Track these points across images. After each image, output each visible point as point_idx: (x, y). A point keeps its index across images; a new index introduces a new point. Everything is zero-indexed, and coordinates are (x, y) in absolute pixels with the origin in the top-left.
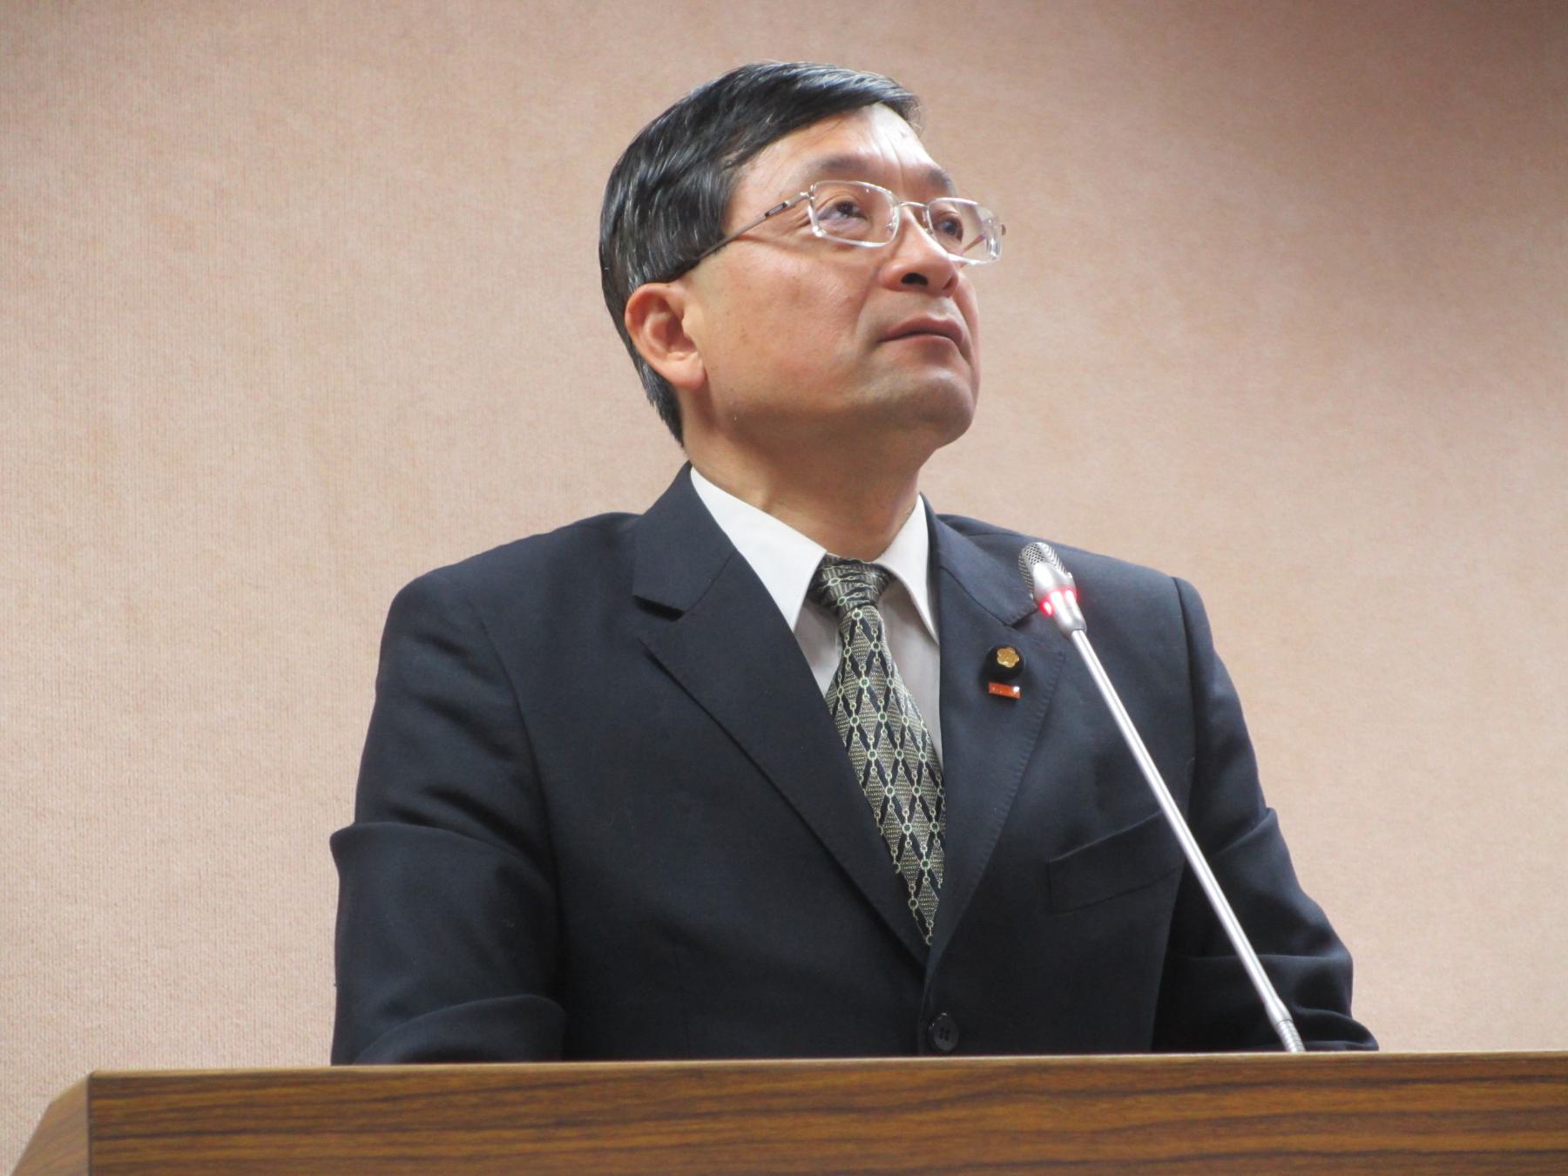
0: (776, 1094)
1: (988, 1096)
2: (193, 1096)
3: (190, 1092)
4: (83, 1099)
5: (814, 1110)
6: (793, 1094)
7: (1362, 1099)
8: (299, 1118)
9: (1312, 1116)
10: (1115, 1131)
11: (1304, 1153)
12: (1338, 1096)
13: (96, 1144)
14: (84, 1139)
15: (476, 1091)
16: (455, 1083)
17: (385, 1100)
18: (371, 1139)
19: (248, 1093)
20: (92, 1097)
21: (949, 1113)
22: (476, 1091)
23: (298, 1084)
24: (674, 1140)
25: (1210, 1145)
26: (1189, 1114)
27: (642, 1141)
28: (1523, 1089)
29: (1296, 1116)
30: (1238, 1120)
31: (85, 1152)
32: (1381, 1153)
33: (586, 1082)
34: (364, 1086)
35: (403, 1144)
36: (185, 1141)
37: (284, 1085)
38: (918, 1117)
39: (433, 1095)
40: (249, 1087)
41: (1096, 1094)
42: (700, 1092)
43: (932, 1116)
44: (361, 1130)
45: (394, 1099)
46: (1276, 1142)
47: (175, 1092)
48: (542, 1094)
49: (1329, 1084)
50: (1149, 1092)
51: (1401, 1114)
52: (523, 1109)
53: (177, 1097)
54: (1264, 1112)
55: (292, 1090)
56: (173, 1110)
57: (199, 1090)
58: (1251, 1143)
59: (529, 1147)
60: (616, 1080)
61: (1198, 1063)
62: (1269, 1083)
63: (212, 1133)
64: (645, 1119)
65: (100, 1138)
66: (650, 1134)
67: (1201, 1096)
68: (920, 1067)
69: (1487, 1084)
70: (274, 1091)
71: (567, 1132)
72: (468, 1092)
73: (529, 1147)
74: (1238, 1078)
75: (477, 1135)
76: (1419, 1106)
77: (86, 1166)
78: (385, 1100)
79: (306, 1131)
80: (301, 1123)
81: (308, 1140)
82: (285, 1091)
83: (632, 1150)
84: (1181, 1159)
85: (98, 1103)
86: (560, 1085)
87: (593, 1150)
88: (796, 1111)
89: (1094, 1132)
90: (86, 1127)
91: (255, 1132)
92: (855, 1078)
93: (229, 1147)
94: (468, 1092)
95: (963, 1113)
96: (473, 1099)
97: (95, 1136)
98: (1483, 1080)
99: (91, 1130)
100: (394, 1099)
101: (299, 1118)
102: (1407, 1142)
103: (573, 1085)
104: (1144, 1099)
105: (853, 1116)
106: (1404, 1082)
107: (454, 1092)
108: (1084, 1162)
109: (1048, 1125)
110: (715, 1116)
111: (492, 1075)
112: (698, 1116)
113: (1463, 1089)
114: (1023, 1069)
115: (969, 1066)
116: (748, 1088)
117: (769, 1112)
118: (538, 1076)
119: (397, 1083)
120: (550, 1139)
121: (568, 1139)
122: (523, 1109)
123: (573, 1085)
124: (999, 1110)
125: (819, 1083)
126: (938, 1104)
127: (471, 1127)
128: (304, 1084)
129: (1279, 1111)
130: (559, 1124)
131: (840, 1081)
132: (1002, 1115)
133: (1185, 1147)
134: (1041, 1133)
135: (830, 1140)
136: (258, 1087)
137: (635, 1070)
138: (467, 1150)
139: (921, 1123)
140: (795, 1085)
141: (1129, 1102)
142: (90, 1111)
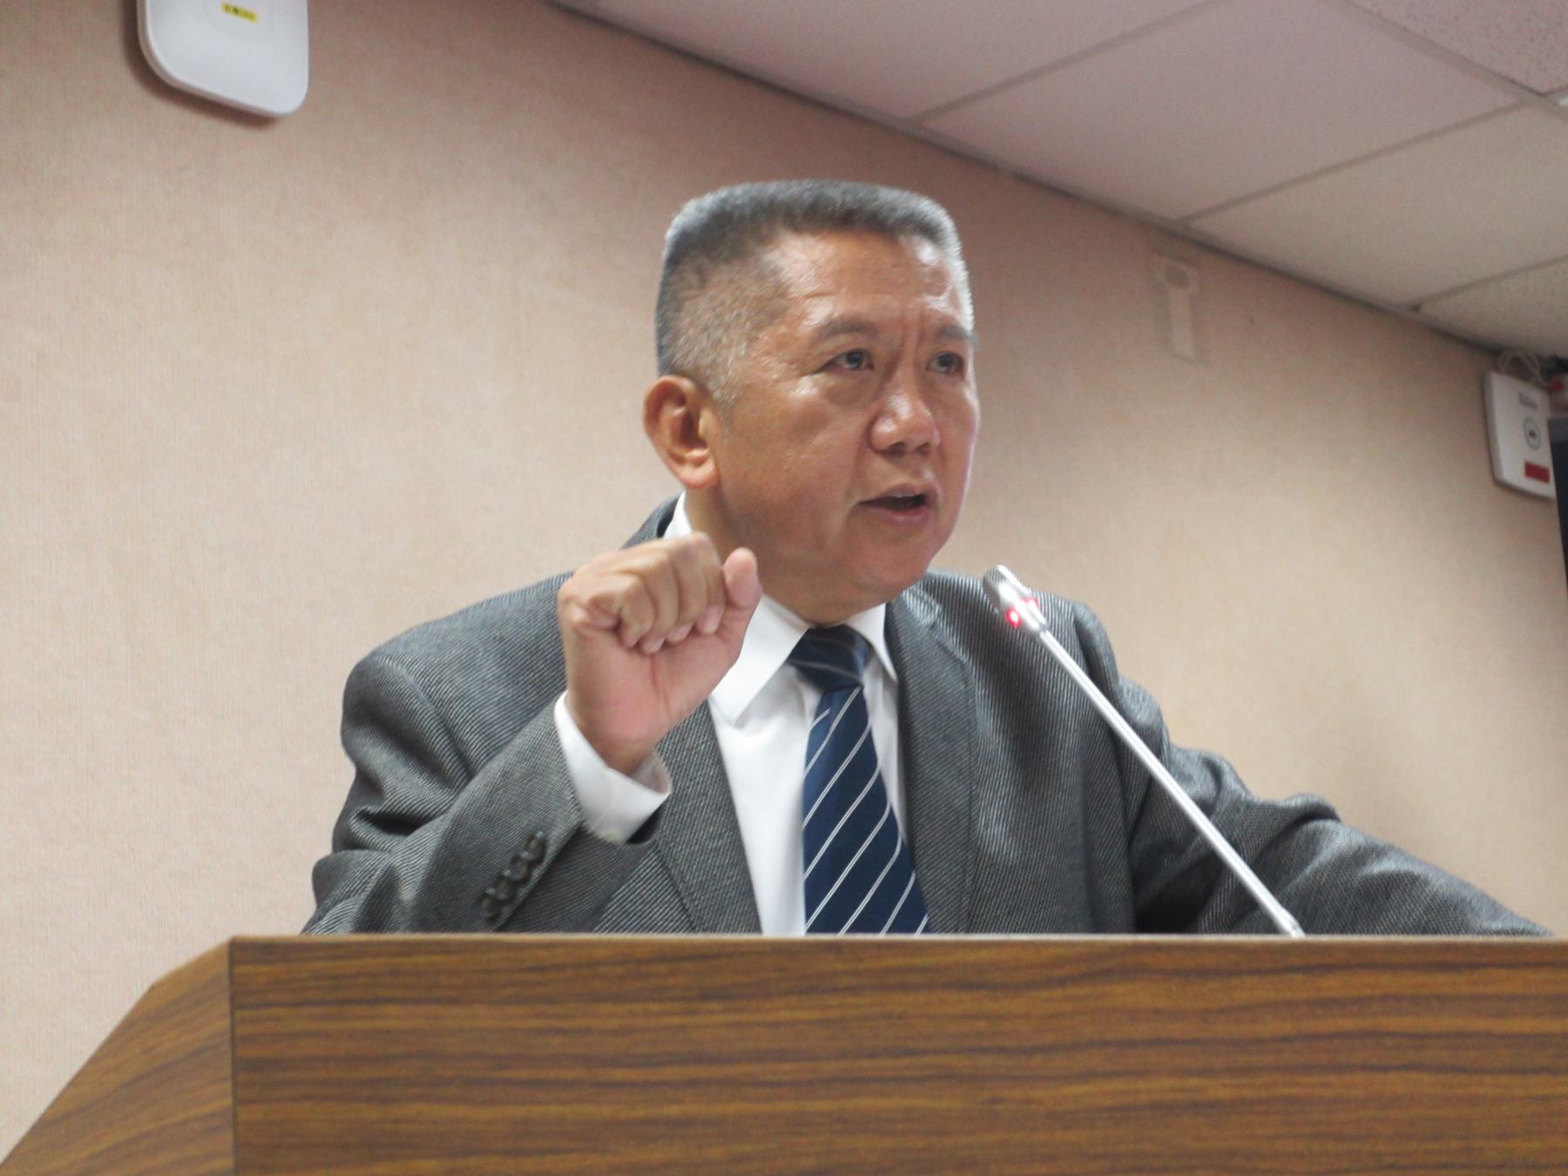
1: (1106, 975)
4: (223, 967)
5: (947, 986)
6: (924, 970)
7: (1442, 982)
9: (1399, 998)
10: (1223, 1011)
11: (1392, 1034)
13: (239, 1014)
14: (225, 1007)
16: (600, 953)
19: (398, 960)
20: (233, 962)
21: (1073, 991)
23: (449, 952)
24: (815, 1015)
25: (1309, 1025)
27: (785, 1015)
29: (1384, 998)
31: (225, 1024)
32: (1460, 1035)
37: (432, 952)
38: (1045, 994)
41: (1204, 973)
42: (839, 966)
43: (1059, 993)
44: (509, 1001)
45: (540, 969)
46: (1366, 1023)
49: (1413, 967)
50: (1251, 972)
51: (1474, 998)
52: (670, 981)
53: (318, 965)
55: (438, 958)
58: (1347, 1024)
59: (676, 1021)
63: (360, 1002)
65: (243, 1007)
67: (1299, 977)
71: (711, 1006)
73: (676, 1021)
76: (1491, 990)
77: (227, 1037)
79: (453, 1001)
83: (776, 1025)
84: (1286, 1039)
85: (240, 969)
87: (738, 1025)
90: (227, 995)
91: (402, 1001)
92: (984, 954)
97: (236, 1004)
99: (232, 999)
102: (1481, 1024)
103: (717, 957)
104: (1248, 980)
108: (1196, 1041)
110: (854, 990)
112: (835, 990)
117: (905, 987)
118: (681, 946)
121: (711, 1012)
122: (670, 981)
126: (1062, 982)
127: (619, 999)
129: (1369, 992)
130: (706, 996)
131: (972, 957)
132: (1122, 994)
133: (1288, 1027)
134: (1157, 1012)
135: (965, 1017)
136: (402, 954)
138: (614, 1023)
141: (1235, 981)
142: (231, 976)
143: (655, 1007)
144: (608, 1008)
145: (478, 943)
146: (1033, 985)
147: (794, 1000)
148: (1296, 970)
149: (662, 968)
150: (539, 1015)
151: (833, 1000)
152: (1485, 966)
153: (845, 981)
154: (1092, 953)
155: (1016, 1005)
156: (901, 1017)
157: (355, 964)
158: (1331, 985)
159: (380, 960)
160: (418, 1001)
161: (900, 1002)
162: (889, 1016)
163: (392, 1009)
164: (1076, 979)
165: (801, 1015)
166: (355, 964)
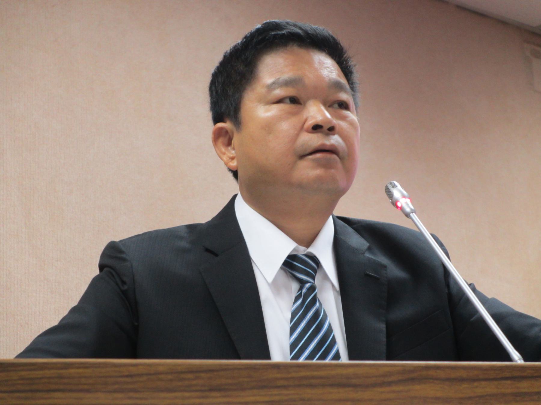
0: (313, 377)
2: (33, 372)
3: (31, 370)
5: (332, 385)
8: (85, 384)
16: (161, 369)
17: (127, 376)
18: (120, 395)
21: (395, 388)
22: (171, 373)
26: (503, 390)
30: (526, 394)
33: (223, 370)
34: (117, 369)
35: (137, 398)
36: (29, 395)
37: (78, 368)
40: (59, 369)
41: (462, 380)
42: (278, 376)
43: (387, 389)
44: (115, 391)
47: (23, 370)
48: (203, 375)
52: (194, 382)
53: (23, 373)
54: (536, 390)
57: (35, 370)
59: (198, 401)
64: (252, 388)
66: (255, 395)
67: (509, 382)
70: (72, 371)
72: (167, 373)
73: (198, 401)
74: (525, 374)
75: (174, 394)
78: (127, 376)
79: (88, 391)
80: (86, 387)
81: (89, 395)
88: (324, 386)
89: (461, 398)
91: (63, 391)
92: (351, 370)
93: (50, 398)
94: (167, 373)
96: (170, 377)
101: (85, 384)
103: (217, 371)
104: (483, 383)
105: (351, 389)
107: (161, 373)
109: (439, 394)
111: (180, 365)
114: (427, 368)
115: (403, 366)
116: (303, 374)
117: (311, 386)
119: (132, 368)
120: (207, 397)
122: (194, 382)
124: (417, 387)
125: (333, 372)
126: (390, 384)
127: (169, 390)
130: (212, 390)
131: (344, 372)
139: (382, 392)
141: (476, 384)
143: (187, 394)
144: (163, 395)
145: (100, 364)
146: (374, 385)
147: (255, 391)
148: (507, 378)
149: (190, 376)
150: (130, 398)
151: (276, 392)
154: (405, 370)
155: (367, 394)
156: (308, 400)
158: (524, 386)
159: (52, 371)
160: (71, 391)
161: (309, 393)
162: (303, 400)
163: (58, 395)
165: (258, 398)
166: (40, 373)
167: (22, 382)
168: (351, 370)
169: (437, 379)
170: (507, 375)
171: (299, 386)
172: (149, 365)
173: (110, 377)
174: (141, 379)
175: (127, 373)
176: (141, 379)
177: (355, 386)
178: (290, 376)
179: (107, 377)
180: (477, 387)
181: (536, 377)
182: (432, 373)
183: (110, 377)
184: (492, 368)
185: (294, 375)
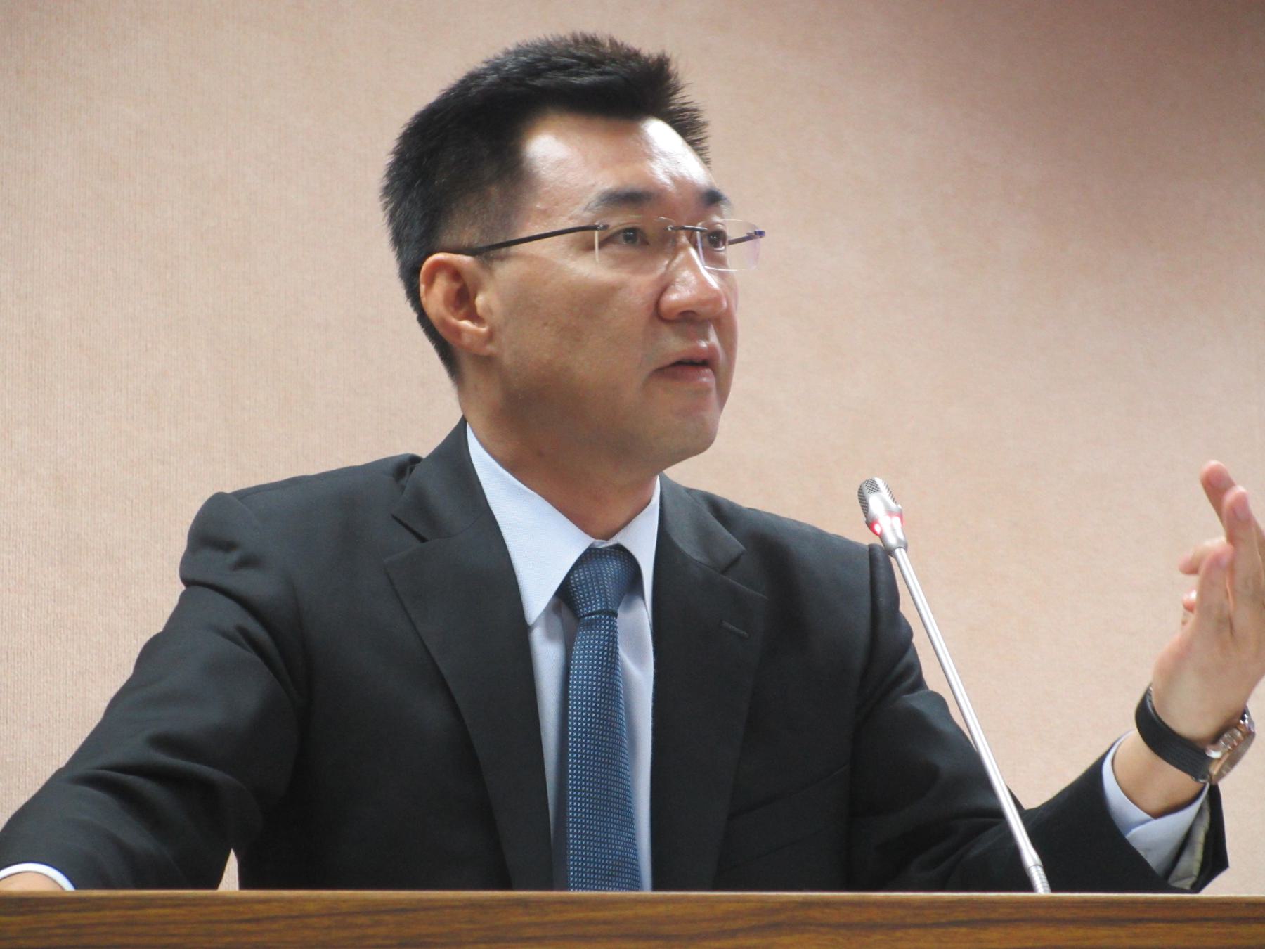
0: (590, 922)
1: (776, 927)
2: (80, 915)
6: (606, 922)
12: (1080, 932)
15: (330, 915)
16: (311, 907)
19: (131, 913)
22: (330, 915)
23: (174, 906)
28: (1243, 930)
33: (425, 909)
34: (231, 908)
37: (163, 906)
39: (294, 917)
42: (526, 919)
43: (730, 943)
45: (257, 921)
47: (66, 911)
48: (387, 918)
52: (370, 932)
53: (64, 916)
56: (63, 927)
60: (453, 907)
61: (960, 902)
62: (1024, 920)
67: (964, 930)
68: (720, 901)
69: (1211, 924)
72: (323, 916)
74: (994, 916)
82: (162, 911)
86: (404, 910)
92: (661, 909)
94: (323, 916)
95: (753, 941)
96: (326, 922)
98: (1207, 920)
100: (257, 921)
103: (415, 910)
104: (913, 932)
106: (1140, 920)
107: (310, 916)
111: (345, 901)
113: (1191, 929)
115: (760, 900)
119: (257, 907)
122: (370, 932)
123: (415, 910)
124: (786, 940)
125: (629, 913)
126: (733, 934)
128: (179, 906)
131: (648, 911)
137: (469, 900)
140: (608, 914)
141: (899, 934)
148: (959, 924)
152: (1150, 920)
153: (529, 932)
157: (94, 916)
159: (116, 913)
164: (750, 931)
166: (94, 916)
167: (59, 931)
168: (661, 909)
169: (822, 925)
170: (962, 916)
171: (564, 938)
172: (291, 901)
173: (221, 922)
174: (275, 926)
175: (246, 917)
176: (275, 926)
177: (667, 937)
178: (546, 919)
179: (211, 922)
180: (901, 939)
181: (1016, 920)
182: (816, 913)
183: (221, 922)
184: (932, 904)
185: (553, 917)
